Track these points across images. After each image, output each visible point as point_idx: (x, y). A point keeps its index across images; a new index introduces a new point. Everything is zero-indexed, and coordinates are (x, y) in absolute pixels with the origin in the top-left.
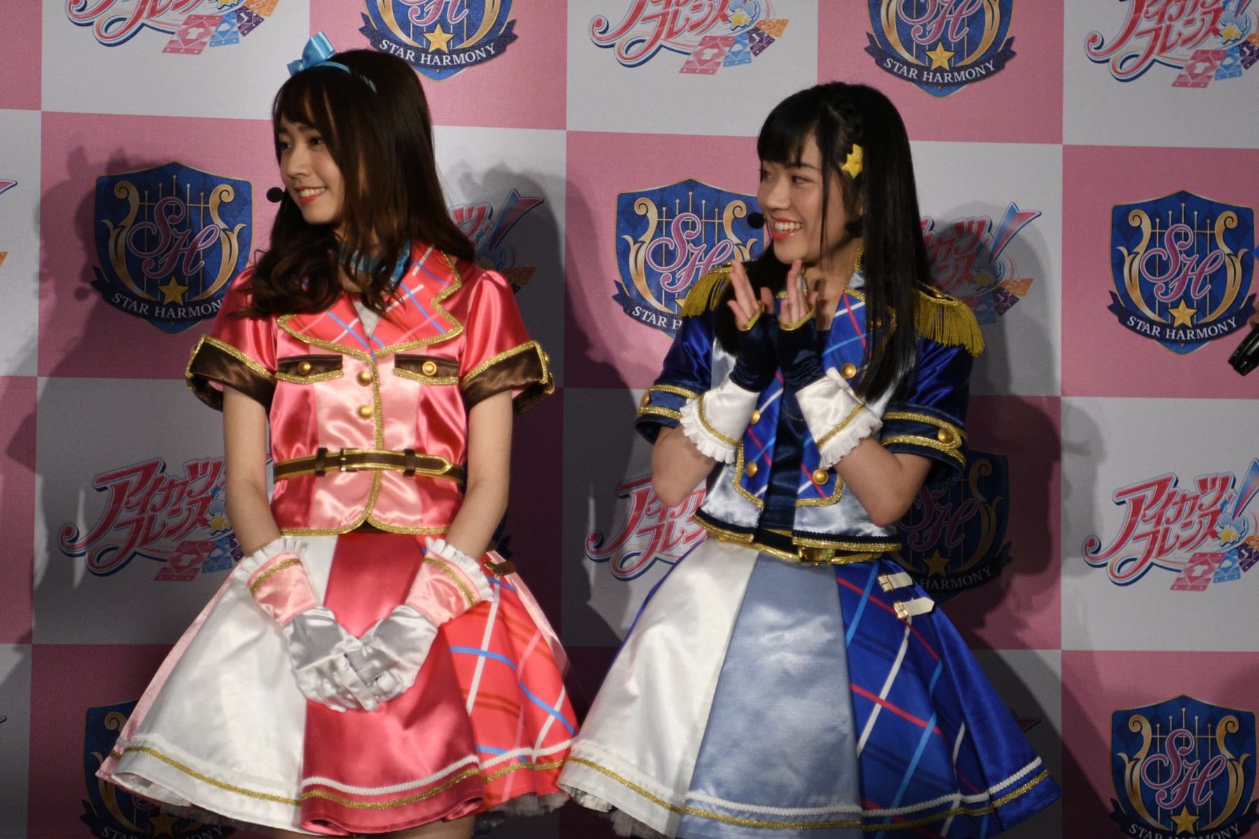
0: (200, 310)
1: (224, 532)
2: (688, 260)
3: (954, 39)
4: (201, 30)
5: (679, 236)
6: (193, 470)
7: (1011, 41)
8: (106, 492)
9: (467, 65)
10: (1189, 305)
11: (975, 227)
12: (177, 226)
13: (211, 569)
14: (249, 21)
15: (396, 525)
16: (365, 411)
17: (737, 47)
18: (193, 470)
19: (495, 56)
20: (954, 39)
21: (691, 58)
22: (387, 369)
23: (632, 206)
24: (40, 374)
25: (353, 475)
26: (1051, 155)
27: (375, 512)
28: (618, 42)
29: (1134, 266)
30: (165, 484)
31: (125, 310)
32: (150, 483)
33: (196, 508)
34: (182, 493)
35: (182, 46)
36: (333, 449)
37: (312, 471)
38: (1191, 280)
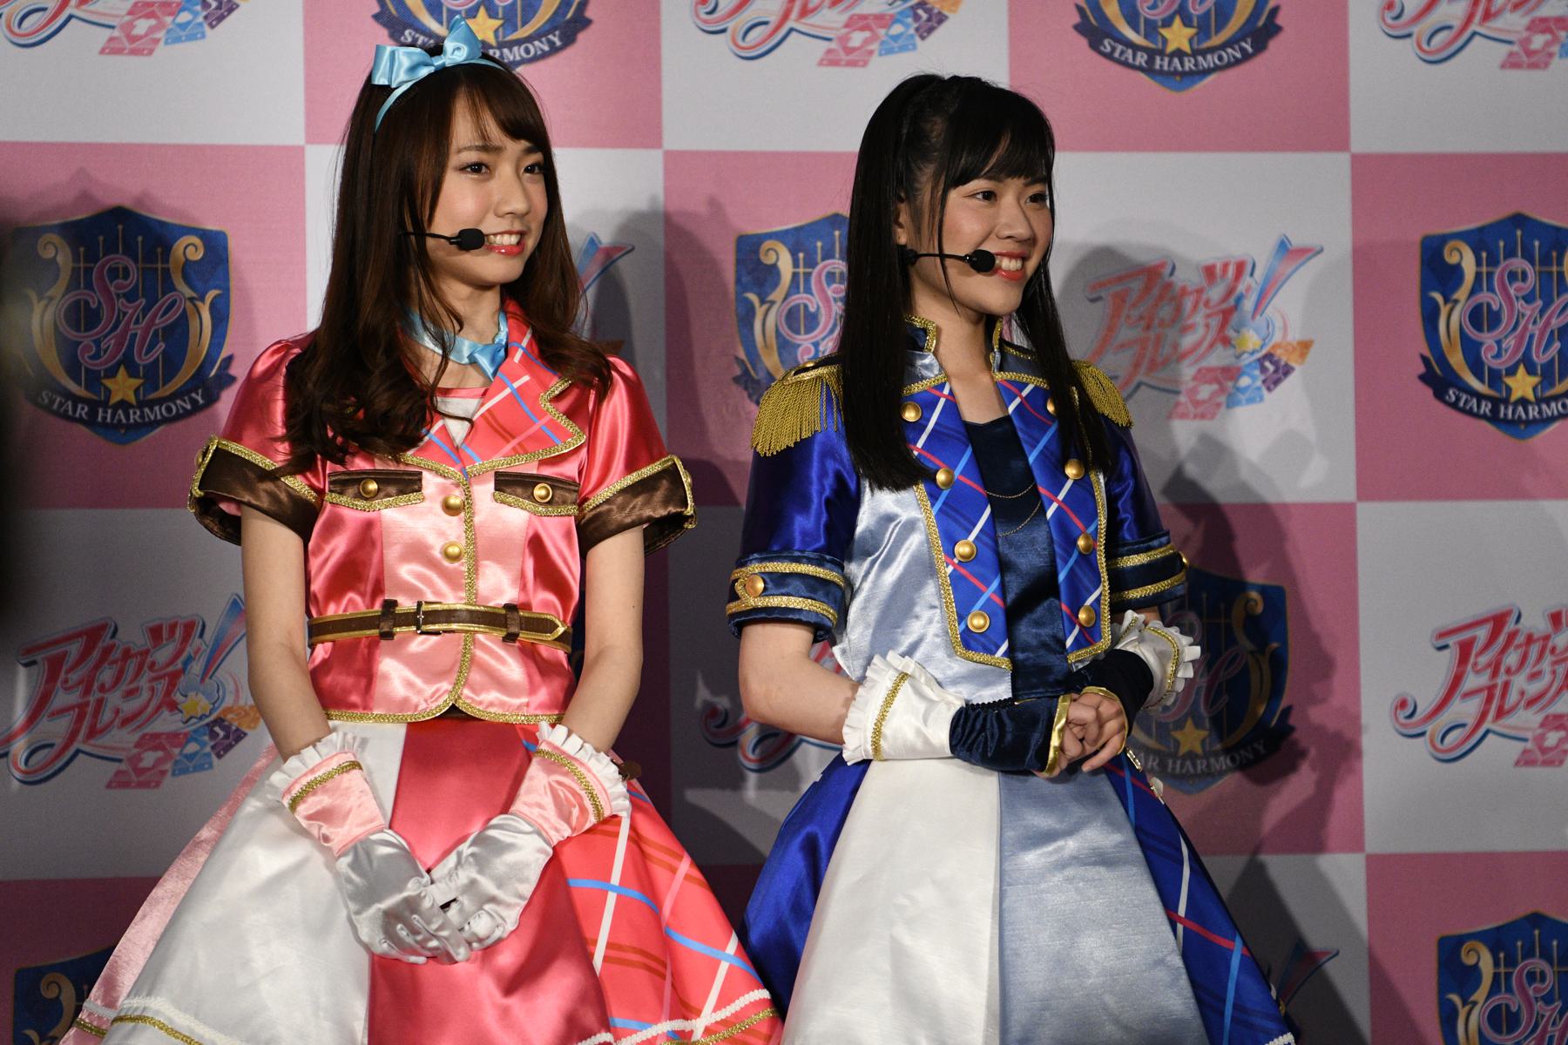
0: (159, 412)
3: (1196, 10)
4: (153, 22)
5: (823, 291)
6: (156, 633)
7: (1275, 11)
10: (1531, 371)
15: (492, 710)
16: (454, 550)
17: (897, 29)
18: (156, 633)
21: (833, 45)
22: (484, 491)
23: (757, 252)
25: (434, 638)
26: (1334, 169)
28: (731, 25)
29: (1453, 319)
32: (96, 655)
33: (161, 686)
36: (406, 604)
37: (375, 632)
38: (1531, 337)
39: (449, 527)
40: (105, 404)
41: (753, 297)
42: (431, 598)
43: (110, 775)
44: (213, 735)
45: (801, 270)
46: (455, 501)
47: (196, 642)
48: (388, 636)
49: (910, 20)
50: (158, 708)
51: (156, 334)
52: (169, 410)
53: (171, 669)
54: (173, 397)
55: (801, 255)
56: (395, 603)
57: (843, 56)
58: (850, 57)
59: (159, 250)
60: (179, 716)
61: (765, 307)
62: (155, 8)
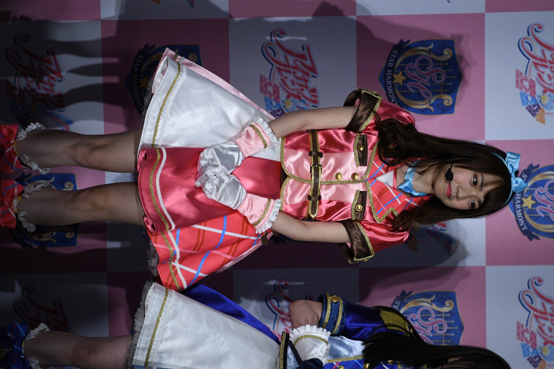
1: (284, 106)
2: (424, 327)
4: (528, 87)
5: (436, 322)
6: (314, 91)
8: (301, 49)
9: (516, 217)
12: (431, 79)
13: (266, 101)
14: (533, 110)
15: (284, 192)
16: (339, 177)
17: (531, 350)
18: (314, 91)
22: (360, 187)
23: (450, 299)
24: (358, 17)
25: (309, 171)
30: (306, 77)
31: (390, 56)
32: (306, 70)
33: (295, 93)
35: (520, 78)
36: (321, 160)
39: (348, 175)
40: (393, 72)
42: (323, 170)
43: (264, 75)
44: (278, 111)
45: (443, 315)
46: (357, 177)
47: (311, 104)
48: (310, 154)
49: (534, 355)
50: (287, 91)
51: (418, 90)
52: (391, 94)
53: (301, 96)
54: (395, 95)
55: (449, 315)
56: (321, 157)
57: (521, 331)
58: (520, 334)
59: (447, 90)
60: (285, 98)
61: (430, 302)
62: (533, 88)
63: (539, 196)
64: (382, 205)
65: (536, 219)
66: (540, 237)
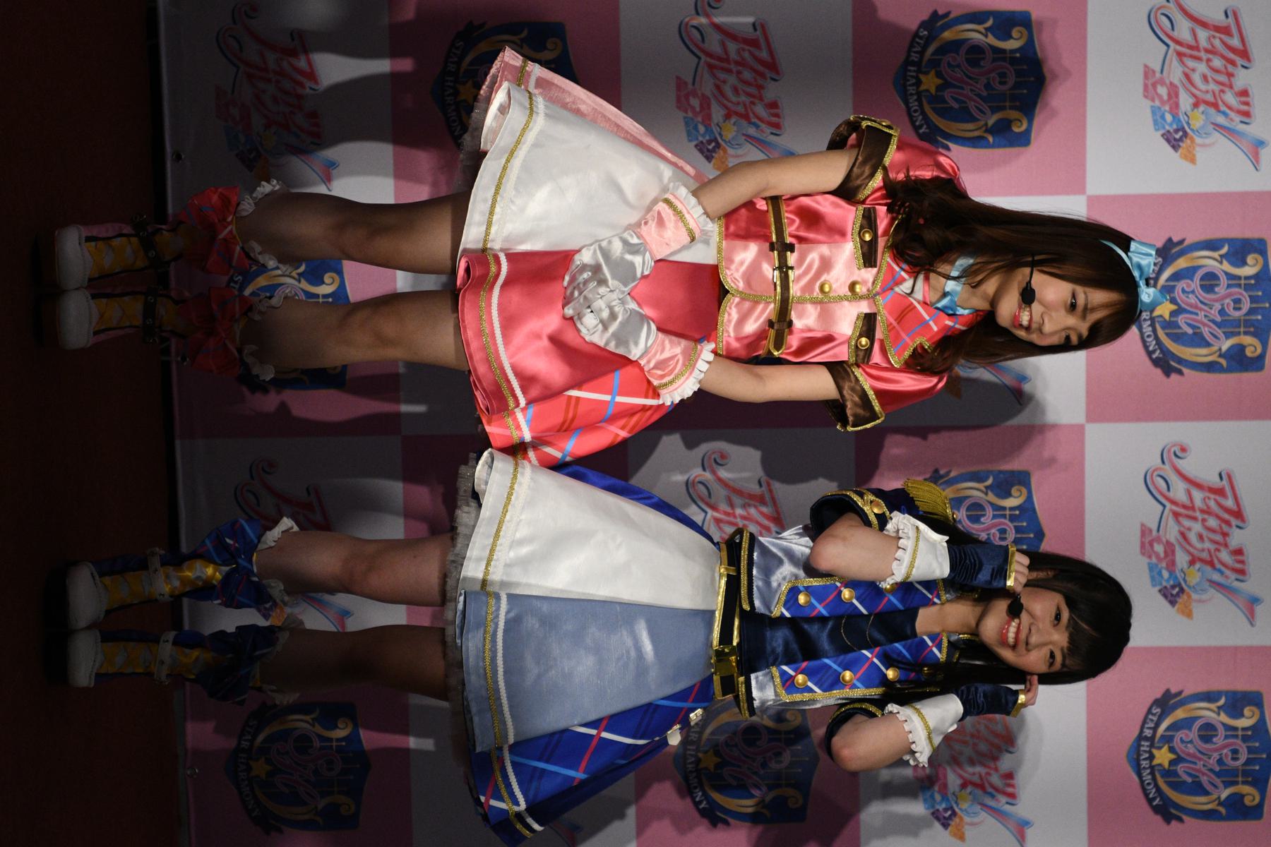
0: (914, 105)
3: (1180, 768)
4: (1165, 97)
6: (773, 105)
11: (1010, 790)
13: (687, 124)
16: (827, 289)
17: (1166, 574)
18: (773, 105)
19: (1151, 358)
20: (1180, 768)
22: (864, 307)
27: (737, 300)
28: (1167, 467)
30: (760, 81)
33: (741, 109)
34: (753, 96)
35: (1151, 80)
36: (792, 259)
37: (774, 238)
39: (840, 285)
40: (919, 71)
41: (989, 482)
44: (709, 142)
46: (858, 288)
47: (768, 130)
48: (772, 248)
52: (915, 111)
56: (792, 251)
57: (1147, 540)
58: (1147, 545)
63: (1183, 296)
64: (903, 334)
65: (1178, 338)
66: (1185, 370)
